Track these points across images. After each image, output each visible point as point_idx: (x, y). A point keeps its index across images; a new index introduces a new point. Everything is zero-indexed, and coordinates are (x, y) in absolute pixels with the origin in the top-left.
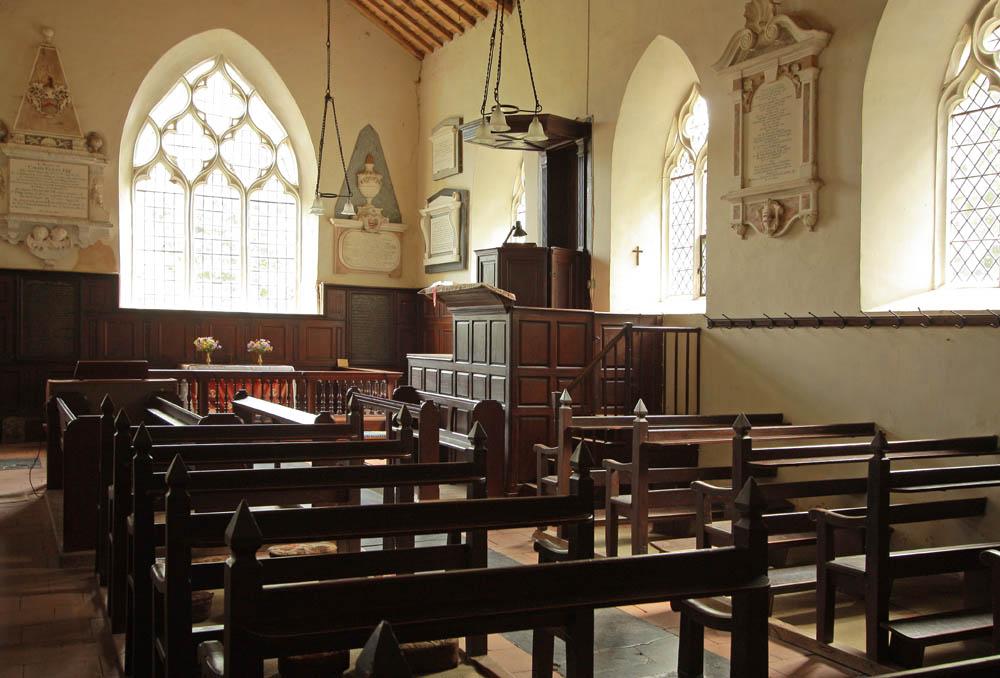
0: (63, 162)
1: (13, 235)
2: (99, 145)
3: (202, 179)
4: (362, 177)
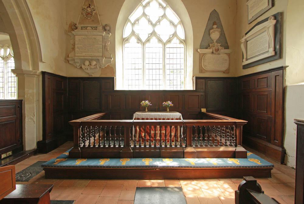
0: (93, 35)
1: (78, 65)
2: (109, 28)
3: (148, 40)
4: (211, 31)
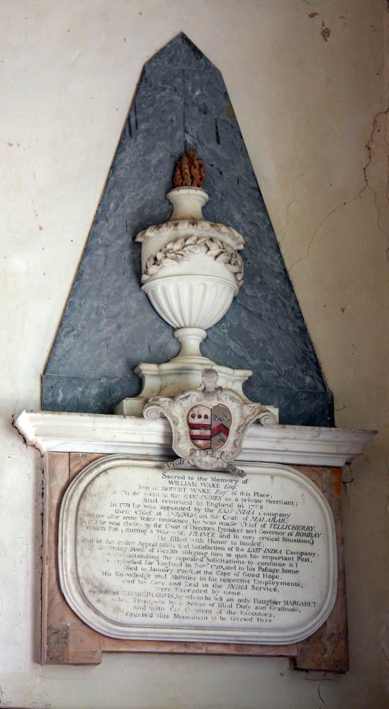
4: (155, 239)
